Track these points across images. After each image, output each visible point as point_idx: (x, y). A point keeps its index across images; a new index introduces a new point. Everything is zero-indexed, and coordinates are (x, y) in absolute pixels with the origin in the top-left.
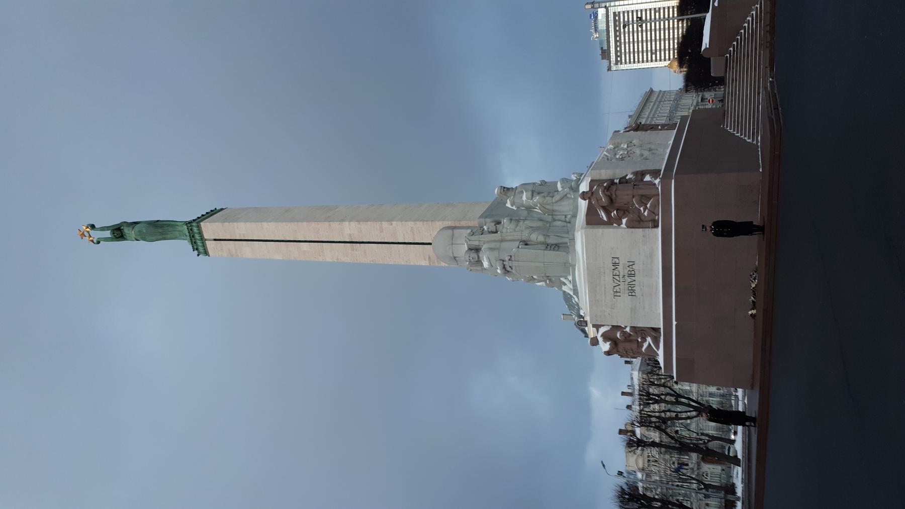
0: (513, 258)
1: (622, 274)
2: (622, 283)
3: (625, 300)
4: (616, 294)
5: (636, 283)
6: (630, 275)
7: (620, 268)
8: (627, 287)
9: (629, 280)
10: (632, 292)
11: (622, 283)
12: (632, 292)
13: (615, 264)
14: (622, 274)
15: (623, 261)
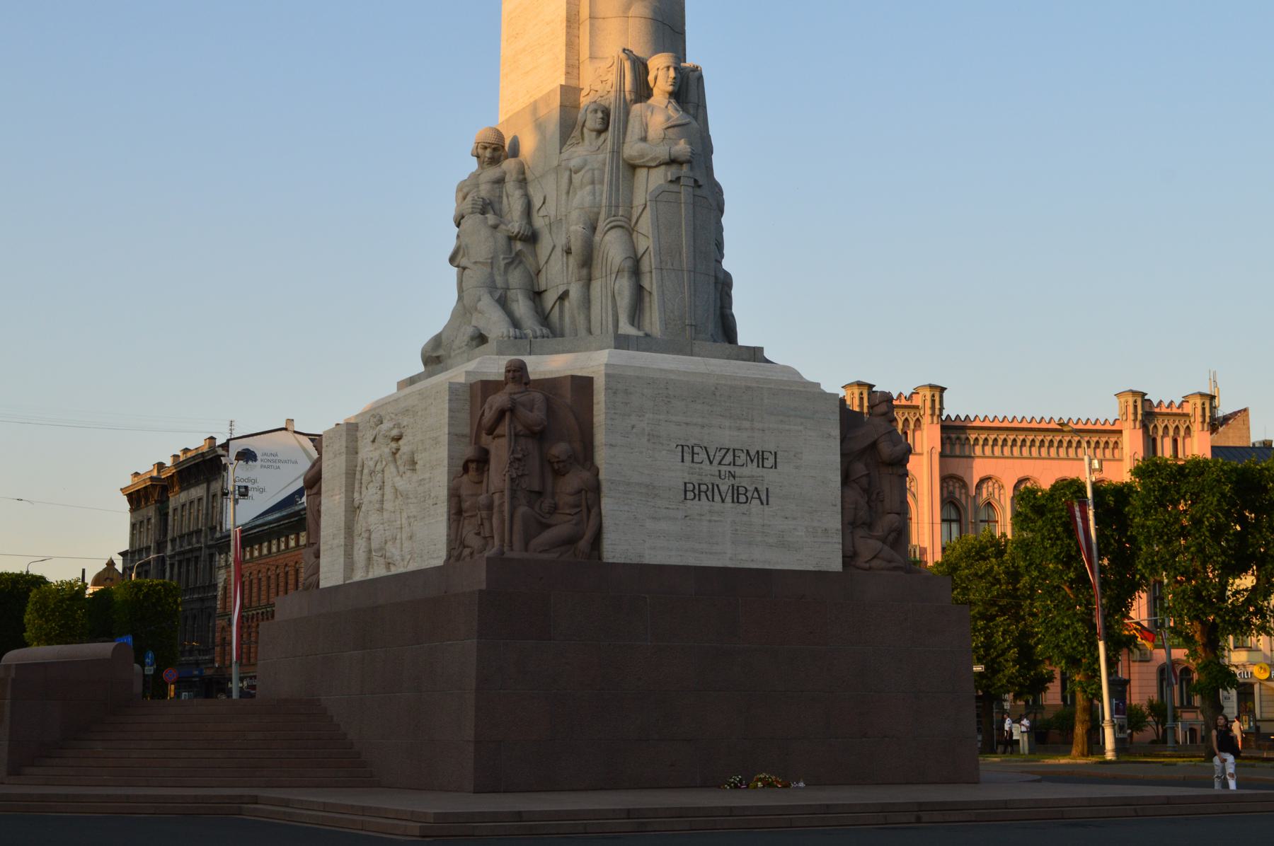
0: (698, 192)
1: (738, 471)
2: (715, 468)
3: (675, 472)
4: (688, 451)
5: (717, 505)
6: (735, 491)
7: (752, 469)
8: (707, 480)
9: (724, 488)
10: (694, 491)
11: (715, 468)
12: (694, 491)
13: (760, 458)
14: (738, 471)
15: (770, 476)
